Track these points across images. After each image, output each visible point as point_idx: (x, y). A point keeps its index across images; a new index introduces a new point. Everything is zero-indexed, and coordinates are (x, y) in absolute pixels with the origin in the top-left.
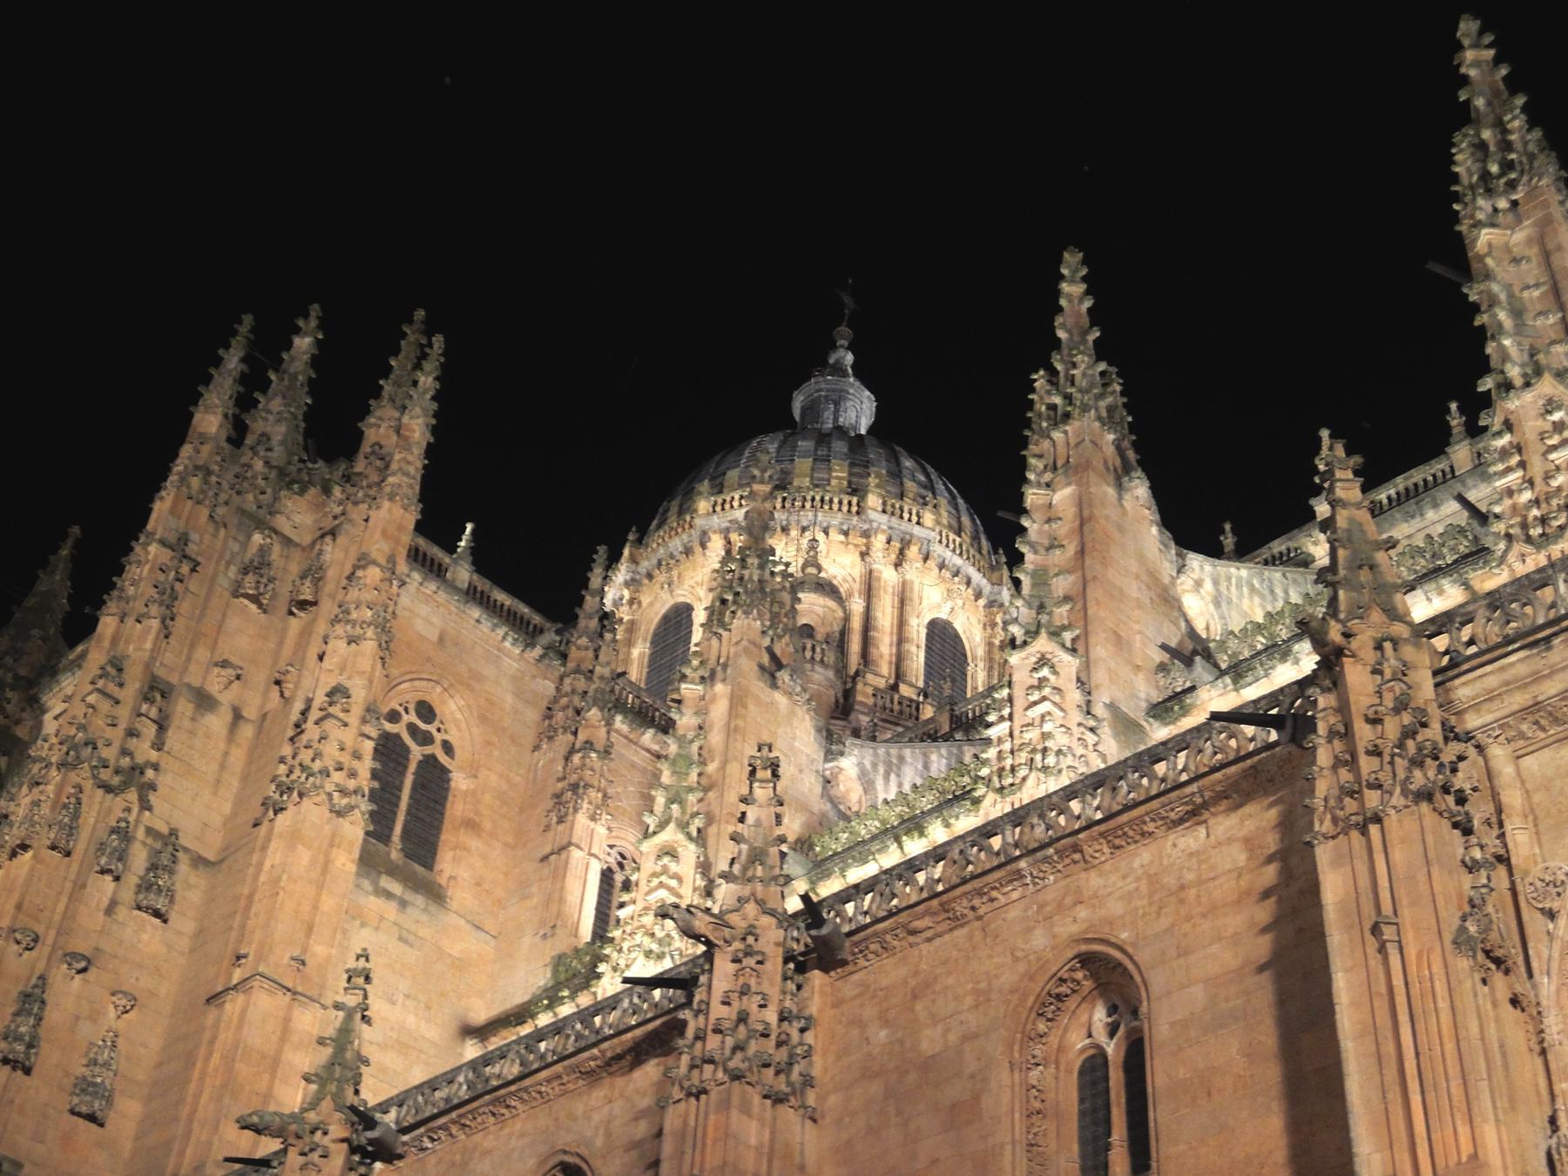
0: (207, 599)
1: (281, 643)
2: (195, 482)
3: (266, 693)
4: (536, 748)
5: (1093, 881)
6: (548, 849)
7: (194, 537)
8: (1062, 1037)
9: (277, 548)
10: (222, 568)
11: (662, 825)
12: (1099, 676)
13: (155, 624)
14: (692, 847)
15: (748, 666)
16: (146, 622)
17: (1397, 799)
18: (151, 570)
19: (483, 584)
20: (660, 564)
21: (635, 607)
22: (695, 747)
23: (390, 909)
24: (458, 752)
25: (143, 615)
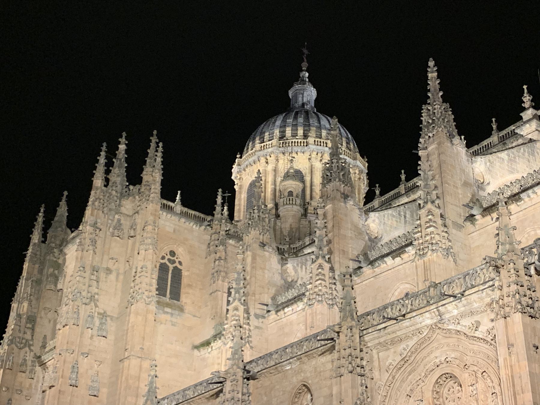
0: (105, 237)
1: (127, 249)
2: (97, 203)
3: (125, 264)
4: (206, 258)
5: (305, 367)
6: (211, 292)
7: (99, 221)
8: (302, 401)
9: (122, 218)
10: (108, 229)
11: (234, 300)
12: (336, 266)
13: (92, 251)
14: (242, 306)
15: (256, 246)
16: (89, 252)
17: (346, 372)
18: (88, 234)
19: (185, 209)
20: (247, 166)
21: (241, 180)
22: (242, 274)
23: (168, 317)
24: (183, 264)
25: (88, 250)
